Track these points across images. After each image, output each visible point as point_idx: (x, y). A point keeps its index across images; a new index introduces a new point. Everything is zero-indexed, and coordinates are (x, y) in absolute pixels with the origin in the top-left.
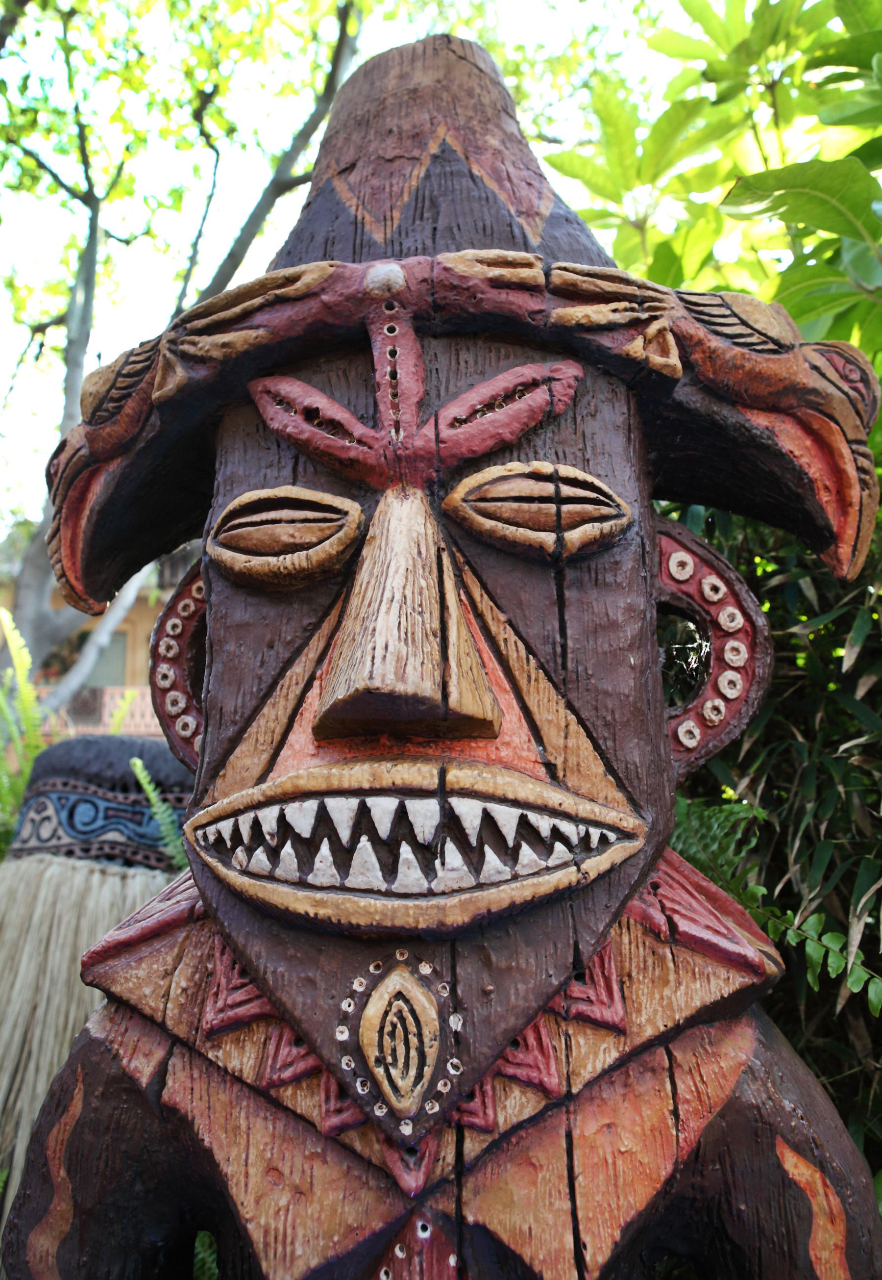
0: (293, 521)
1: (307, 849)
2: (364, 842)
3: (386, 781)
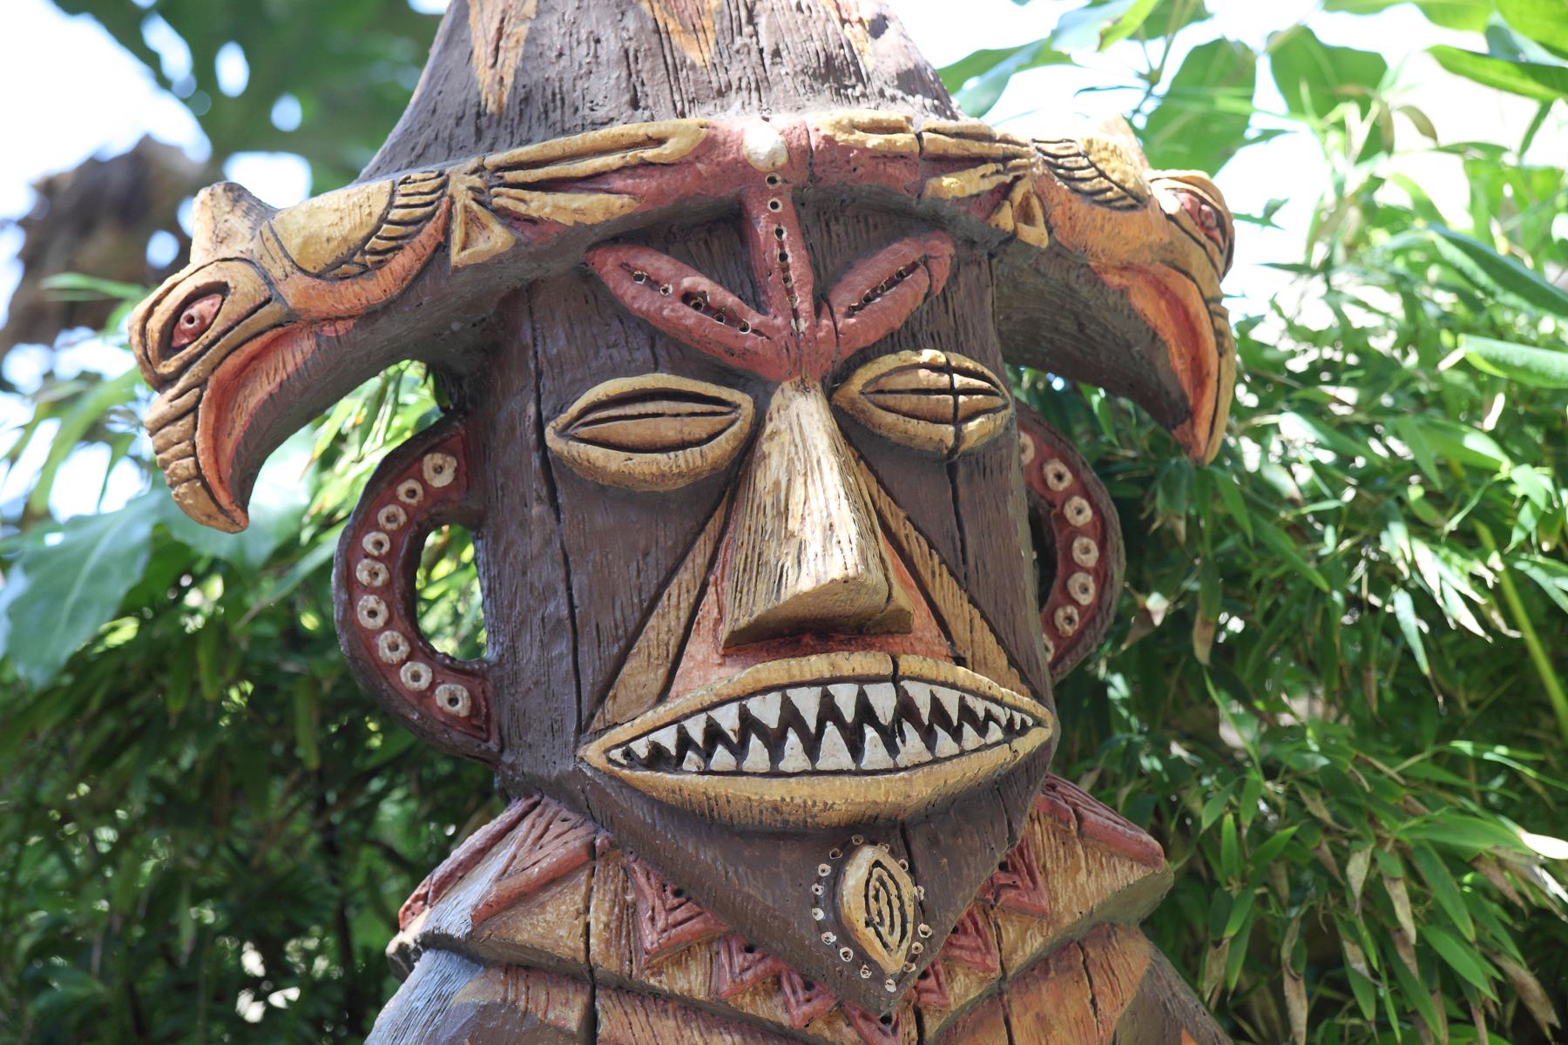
1: (775, 743)
2: (830, 727)
3: (847, 672)
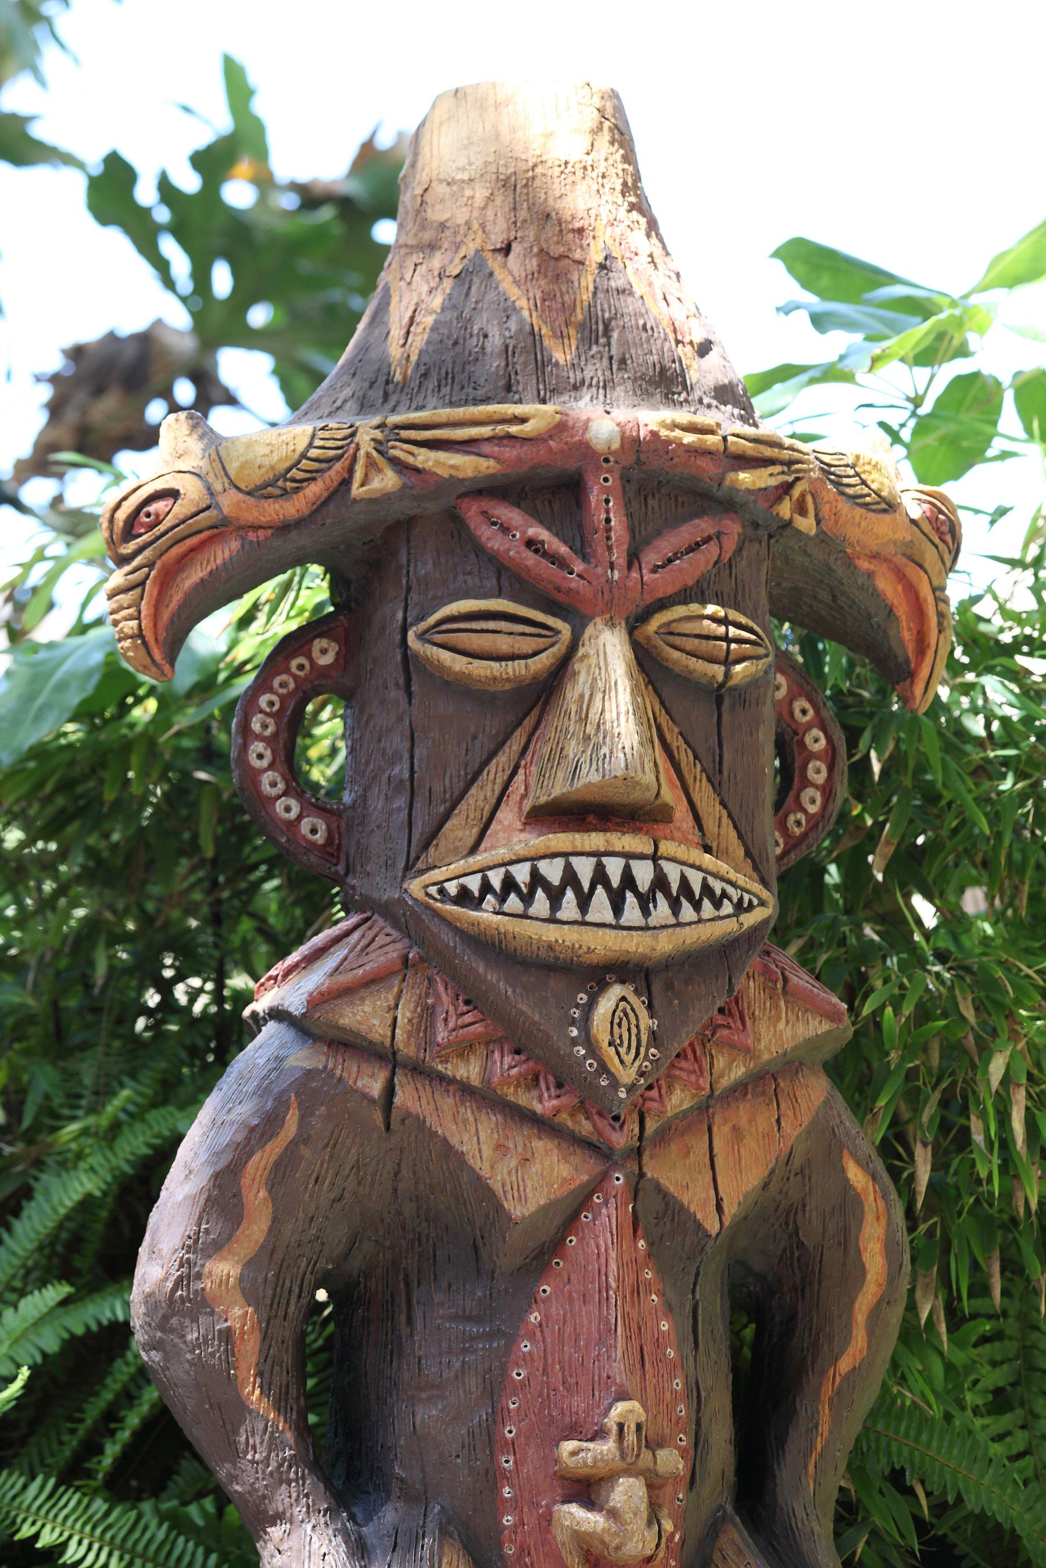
1: (555, 897)
2: (600, 890)
3: (618, 848)
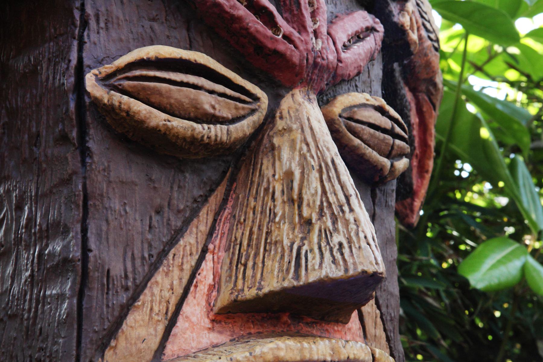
0: (211, 92)
